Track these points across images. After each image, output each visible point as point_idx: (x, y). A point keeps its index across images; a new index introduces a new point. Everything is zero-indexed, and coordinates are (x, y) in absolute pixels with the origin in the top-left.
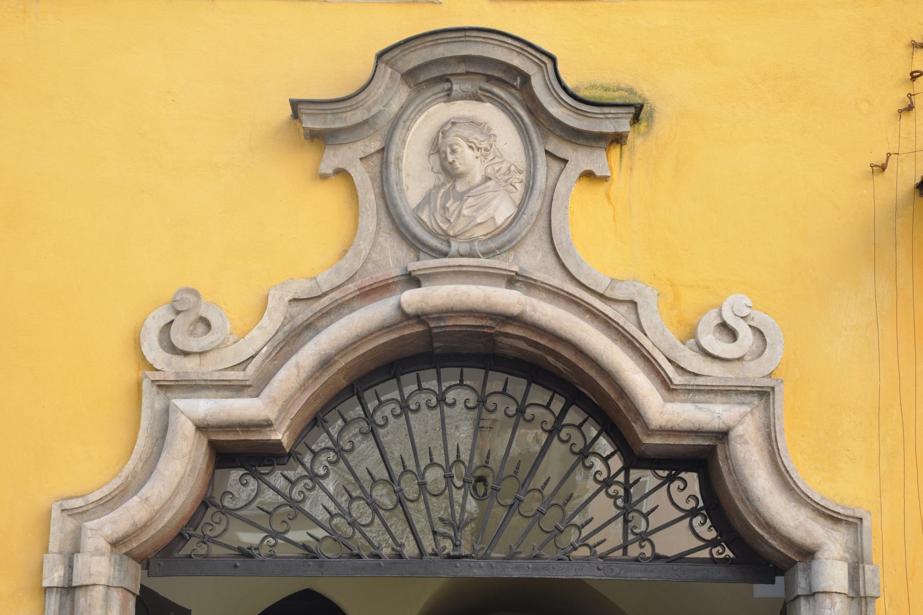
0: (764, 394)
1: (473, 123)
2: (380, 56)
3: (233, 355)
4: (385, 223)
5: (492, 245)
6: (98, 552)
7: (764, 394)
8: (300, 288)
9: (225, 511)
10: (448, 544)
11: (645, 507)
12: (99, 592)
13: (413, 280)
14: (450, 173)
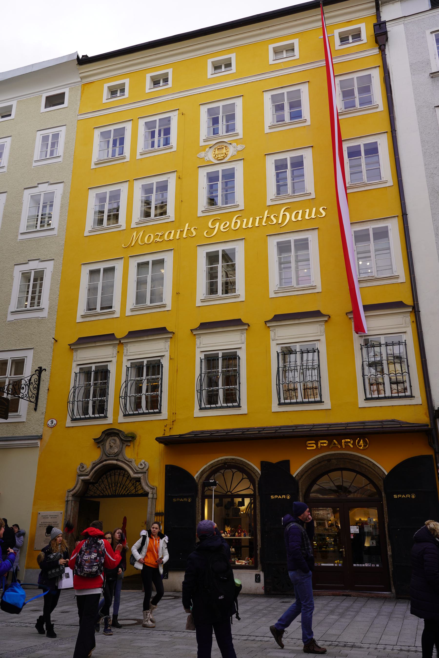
0: (145, 472)
1: (114, 440)
2: (102, 432)
3: (86, 471)
4: (104, 453)
5: (115, 455)
6: (71, 496)
7: (145, 472)
8: (94, 462)
9: (90, 490)
10: (114, 493)
11: (137, 487)
12: (70, 501)
13: (106, 460)
14: (111, 447)
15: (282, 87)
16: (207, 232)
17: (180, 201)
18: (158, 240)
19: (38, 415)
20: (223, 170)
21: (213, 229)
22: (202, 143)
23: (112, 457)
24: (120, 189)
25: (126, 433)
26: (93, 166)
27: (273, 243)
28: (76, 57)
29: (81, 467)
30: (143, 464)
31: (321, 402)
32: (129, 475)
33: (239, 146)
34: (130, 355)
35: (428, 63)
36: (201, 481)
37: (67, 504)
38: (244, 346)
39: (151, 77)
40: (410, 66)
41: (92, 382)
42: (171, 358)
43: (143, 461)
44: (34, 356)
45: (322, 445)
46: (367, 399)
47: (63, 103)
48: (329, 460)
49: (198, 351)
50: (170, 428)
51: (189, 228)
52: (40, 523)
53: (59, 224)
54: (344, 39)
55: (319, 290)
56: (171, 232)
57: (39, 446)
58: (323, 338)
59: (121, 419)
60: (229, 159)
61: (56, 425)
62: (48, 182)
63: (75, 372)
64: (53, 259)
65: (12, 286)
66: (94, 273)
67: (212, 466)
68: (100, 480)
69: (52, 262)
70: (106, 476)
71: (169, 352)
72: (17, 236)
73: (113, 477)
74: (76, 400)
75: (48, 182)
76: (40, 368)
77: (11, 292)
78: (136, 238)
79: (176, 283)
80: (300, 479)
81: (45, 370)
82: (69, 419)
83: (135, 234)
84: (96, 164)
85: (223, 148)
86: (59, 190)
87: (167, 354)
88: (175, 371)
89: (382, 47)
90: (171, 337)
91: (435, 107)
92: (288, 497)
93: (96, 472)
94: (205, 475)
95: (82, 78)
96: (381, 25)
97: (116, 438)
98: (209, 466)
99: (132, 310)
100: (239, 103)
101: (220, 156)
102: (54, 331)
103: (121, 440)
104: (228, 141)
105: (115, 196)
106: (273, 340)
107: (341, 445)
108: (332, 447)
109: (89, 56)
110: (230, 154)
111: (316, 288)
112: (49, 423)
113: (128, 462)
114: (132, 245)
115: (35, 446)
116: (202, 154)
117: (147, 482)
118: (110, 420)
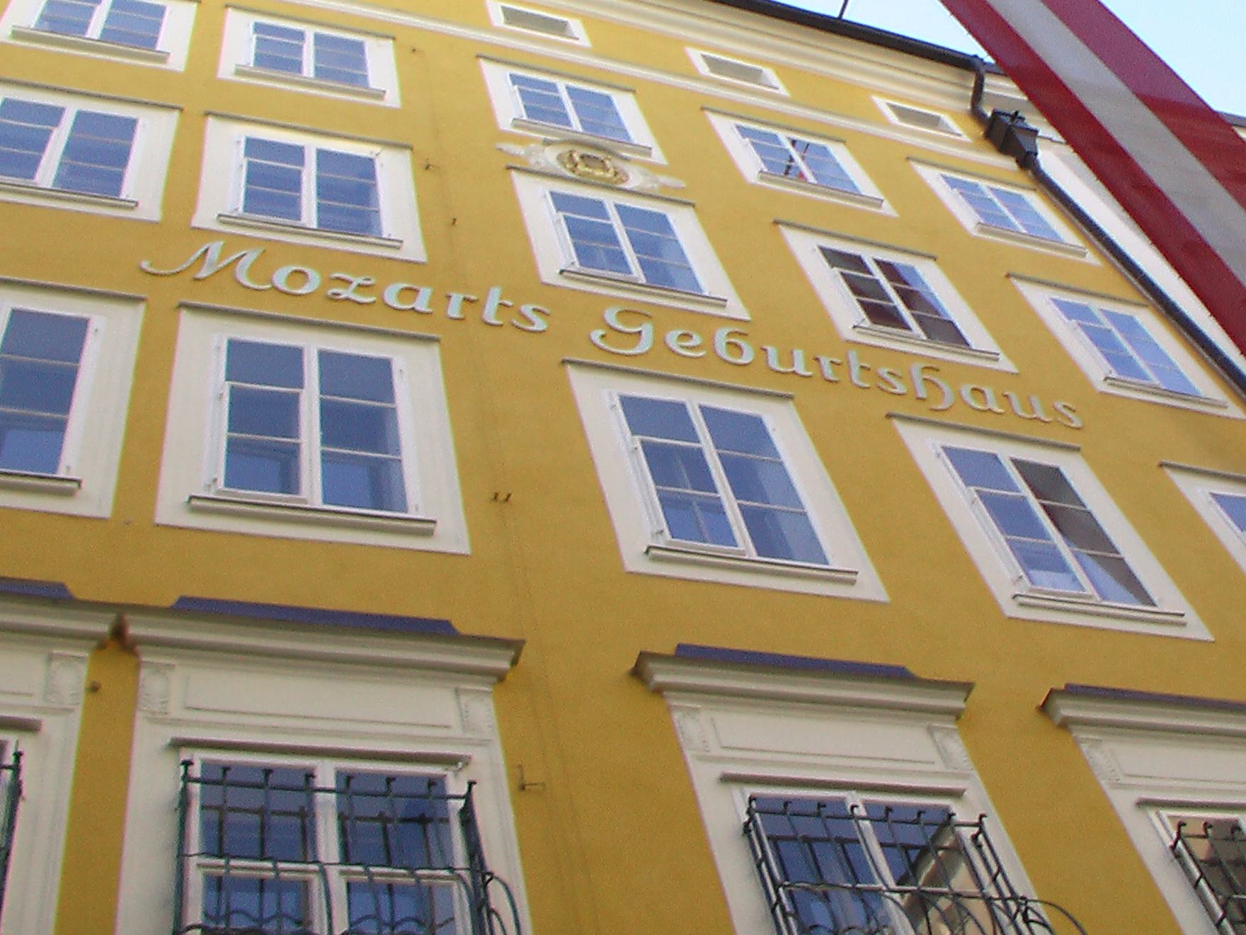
16: (603, 336)
18: (345, 293)
21: (633, 338)
42: (527, 779)
78: (221, 258)
111: (1184, 625)
114: (203, 274)
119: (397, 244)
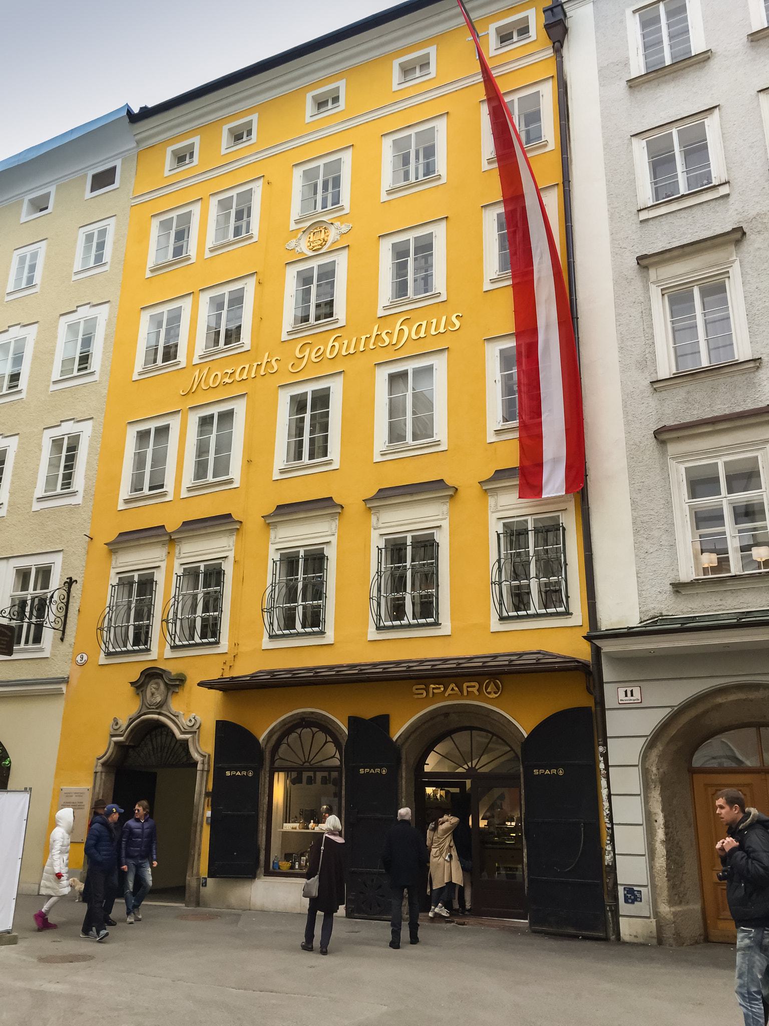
0: (196, 732)
2: (141, 673)
7: (196, 732)
13: (145, 714)
15: (409, 126)
17: (259, 319)
18: (227, 380)
19: (65, 648)
20: (319, 266)
22: (293, 226)
23: (153, 709)
24: (181, 307)
25: (173, 674)
26: (148, 274)
27: (382, 376)
28: (125, 113)
29: (115, 724)
30: (193, 720)
31: (436, 624)
32: (173, 735)
33: (343, 226)
34: (184, 557)
35: (626, 64)
36: (270, 745)
37: (96, 777)
38: (334, 540)
39: (230, 130)
40: (599, 71)
41: (134, 598)
43: (194, 714)
44: (63, 562)
45: (435, 691)
46: (502, 618)
47: (114, 183)
48: (446, 715)
49: (272, 548)
50: (230, 666)
51: (269, 360)
52: (62, 803)
53: (102, 365)
54: (505, 38)
55: (443, 447)
56: (244, 368)
57: (64, 692)
58: (445, 524)
59: (168, 653)
60: (329, 247)
61: (86, 662)
62: (89, 303)
63: (111, 584)
64: (92, 418)
65: (40, 460)
66: (143, 436)
67: (284, 723)
68: (143, 743)
69: (90, 422)
70: (151, 736)
71: (233, 550)
72: (49, 386)
73: (159, 738)
74: (113, 625)
75: (89, 303)
76: (71, 578)
77: (38, 469)
79: (248, 447)
80: (403, 744)
81: (76, 581)
82: (102, 655)
83: (197, 373)
84: (152, 271)
85: (321, 231)
86: (103, 314)
87: (231, 555)
88: (240, 580)
89: (557, 44)
90: (238, 529)
91: (631, 136)
92: (384, 772)
93: (132, 730)
94: (275, 737)
95: (138, 142)
96: (555, 10)
97: (160, 681)
98: (280, 723)
99: (190, 489)
100: (347, 157)
101: (316, 244)
102: (89, 524)
103: (166, 684)
104: (328, 220)
105: (175, 318)
106: (375, 529)
107: (461, 691)
108: (449, 694)
109: (150, 105)
110: (330, 240)
112: (78, 658)
113: (174, 717)
114: (193, 391)
115: (59, 694)
116: (292, 244)
117: (198, 746)
118: (154, 655)
119: (242, 345)
